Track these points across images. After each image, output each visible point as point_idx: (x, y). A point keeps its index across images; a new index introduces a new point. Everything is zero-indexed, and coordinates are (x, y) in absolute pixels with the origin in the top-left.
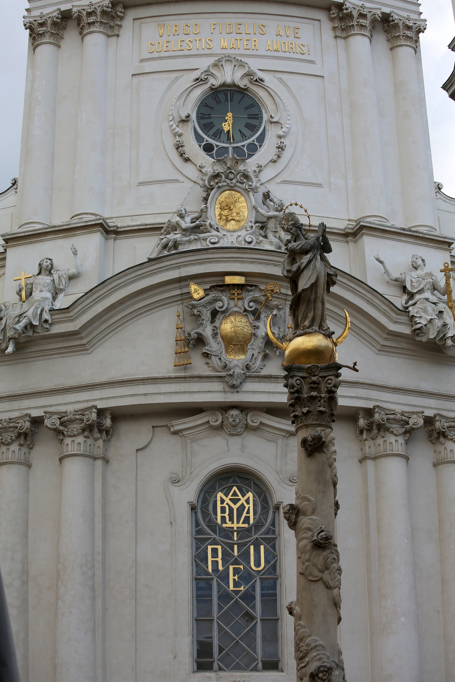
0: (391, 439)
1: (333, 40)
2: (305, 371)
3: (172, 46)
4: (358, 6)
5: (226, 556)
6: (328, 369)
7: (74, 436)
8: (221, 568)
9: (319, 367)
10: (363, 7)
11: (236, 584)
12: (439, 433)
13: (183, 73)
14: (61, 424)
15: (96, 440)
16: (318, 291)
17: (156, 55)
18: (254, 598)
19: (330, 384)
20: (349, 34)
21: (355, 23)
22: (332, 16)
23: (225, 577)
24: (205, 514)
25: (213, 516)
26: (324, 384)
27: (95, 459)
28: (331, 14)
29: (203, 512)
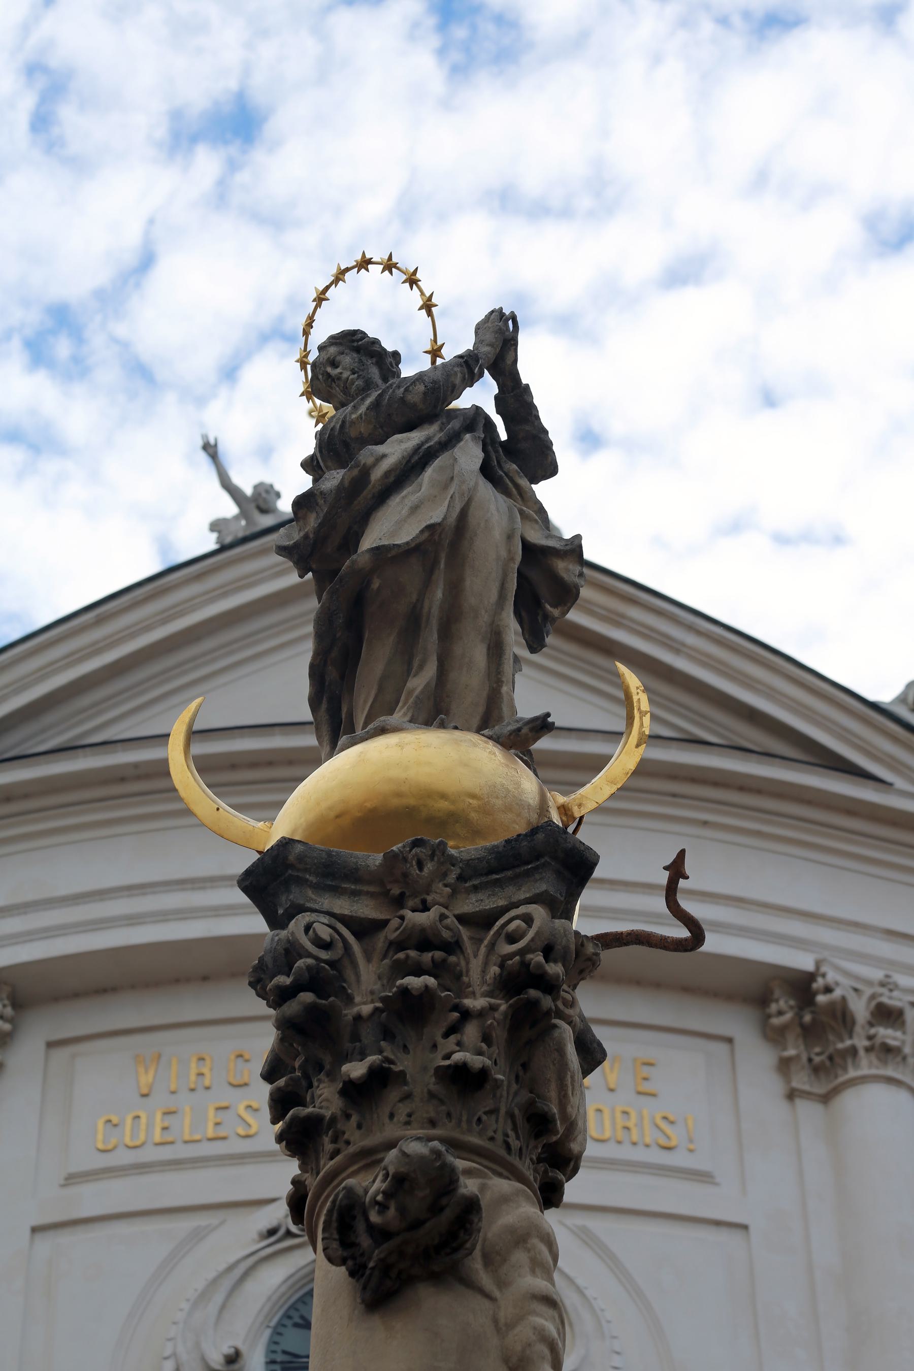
1: (783, 1106)
2: (371, 889)
3: (185, 1126)
4: (869, 983)
6: (509, 873)
9: (453, 861)
10: (889, 983)
13: (221, 1214)
16: (468, 583)
17: (124, 1158)
19: (512, 939)
20: (841, 1079)
21: (860, 1042)
22: (776, 1021)
26: (483, 949)
28: (769, 1016)
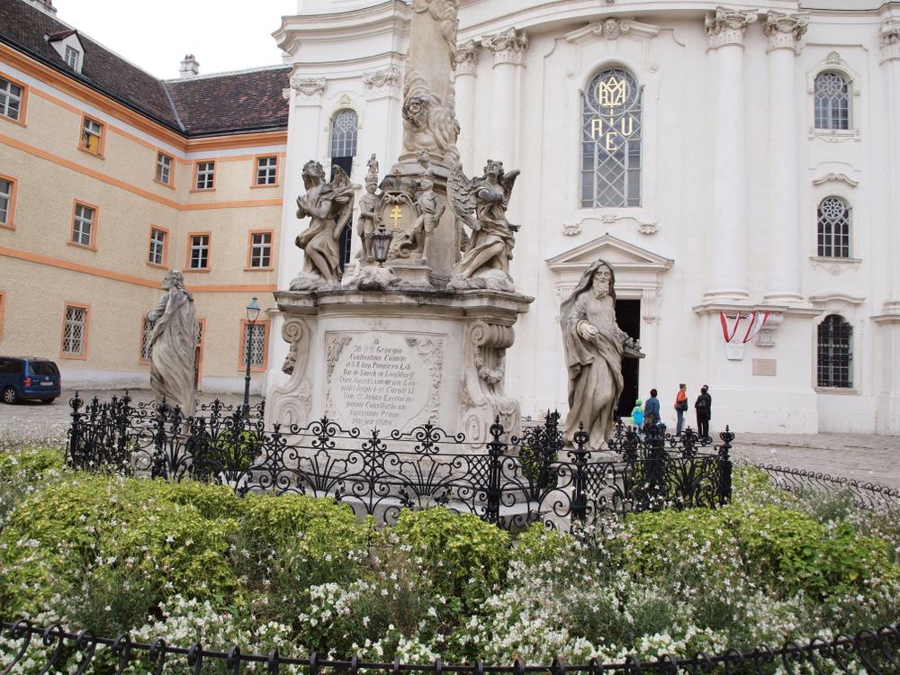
0: (730, 32)
5: (605, 127)
7: (501, 50)
8: (601, 135)
11: (611, 146)
12: (771, 26)
14: (493, 43)
15: (517, 52)
18: (623, 155)
23: (603, 141)
24: (591, 98)
25: (596, 99)
27: (516, 65)
29: (589, 97)
